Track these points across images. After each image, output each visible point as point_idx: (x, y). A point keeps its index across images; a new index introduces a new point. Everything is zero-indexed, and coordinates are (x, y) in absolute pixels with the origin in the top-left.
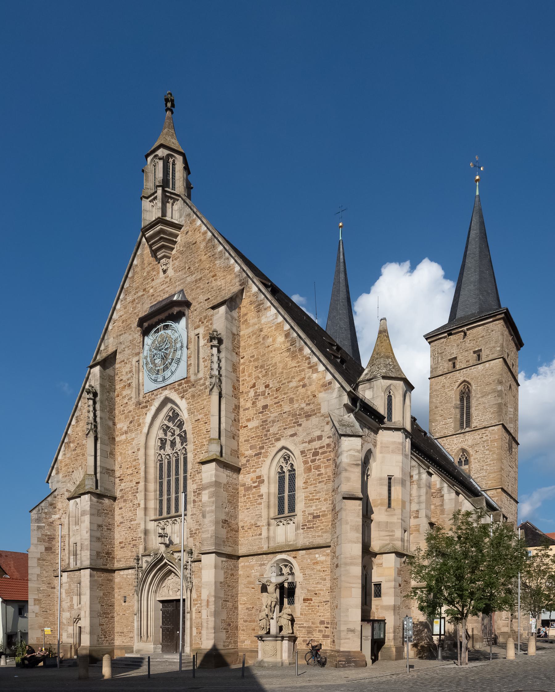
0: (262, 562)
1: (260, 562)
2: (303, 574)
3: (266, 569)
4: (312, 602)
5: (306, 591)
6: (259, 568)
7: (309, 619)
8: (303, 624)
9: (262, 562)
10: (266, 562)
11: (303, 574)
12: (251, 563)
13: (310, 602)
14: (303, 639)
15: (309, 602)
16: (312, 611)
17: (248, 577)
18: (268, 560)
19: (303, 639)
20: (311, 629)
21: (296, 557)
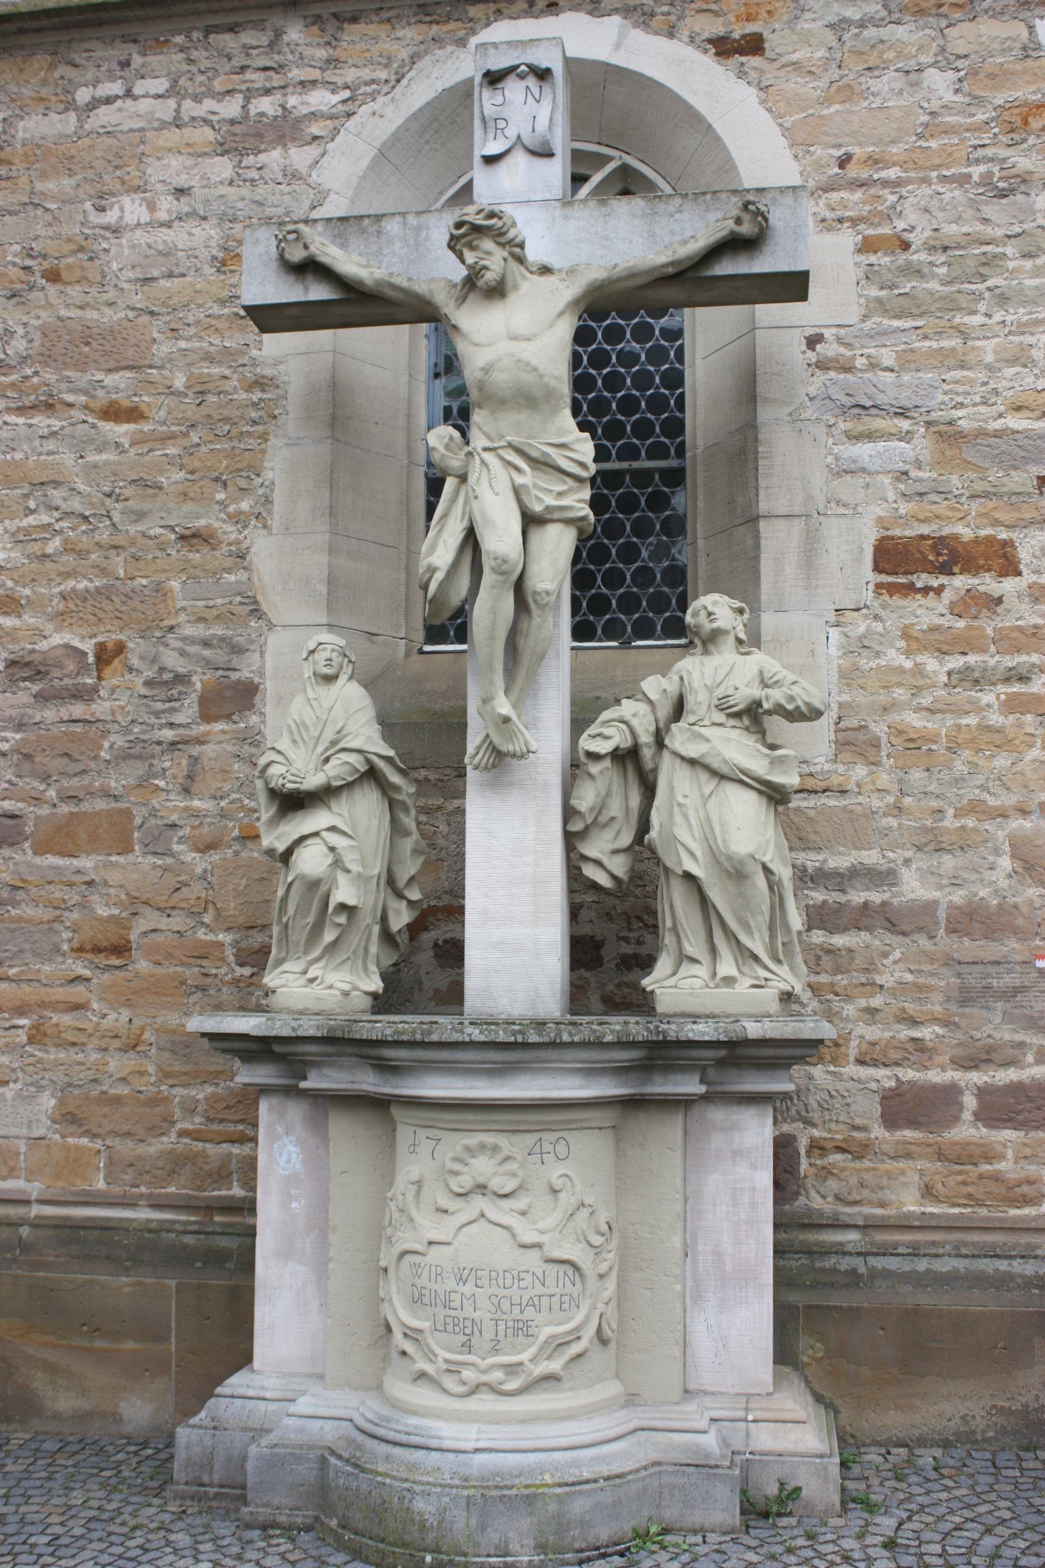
0: (266, 105)
1: (231, 108)
2: (868, 246)
3: (323, 177)
4: (1009, 586)
5: (921, 446)
6: (222, 167)
7: (976, 808)
8: (885, 877)
9: (266, 105)
10: (321, 99)
11: (868, 246)
12: (104, 116)
13: (988, 583)
14: (885, 1077)
15: (960, 582)
16: (1012, 705)
17: (53, 276)
18: (350, 75)
19: (885, 1077)
20: (1012, 947)
21: (754, 45)
